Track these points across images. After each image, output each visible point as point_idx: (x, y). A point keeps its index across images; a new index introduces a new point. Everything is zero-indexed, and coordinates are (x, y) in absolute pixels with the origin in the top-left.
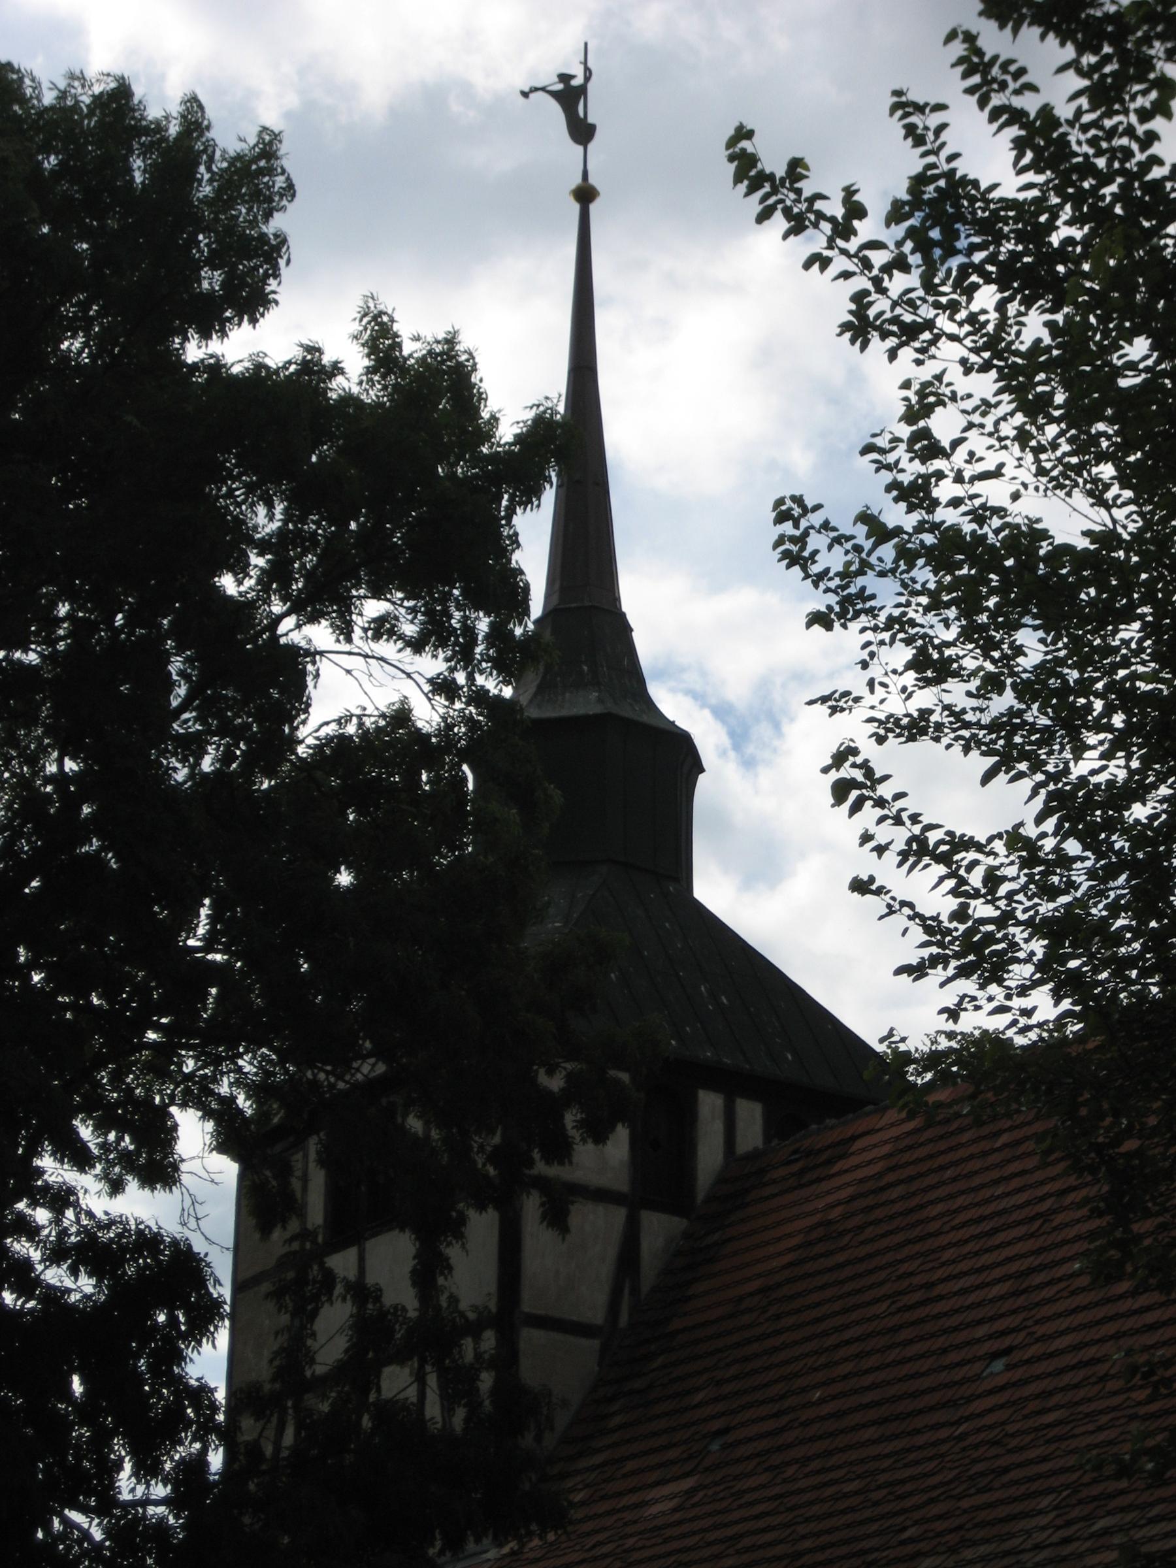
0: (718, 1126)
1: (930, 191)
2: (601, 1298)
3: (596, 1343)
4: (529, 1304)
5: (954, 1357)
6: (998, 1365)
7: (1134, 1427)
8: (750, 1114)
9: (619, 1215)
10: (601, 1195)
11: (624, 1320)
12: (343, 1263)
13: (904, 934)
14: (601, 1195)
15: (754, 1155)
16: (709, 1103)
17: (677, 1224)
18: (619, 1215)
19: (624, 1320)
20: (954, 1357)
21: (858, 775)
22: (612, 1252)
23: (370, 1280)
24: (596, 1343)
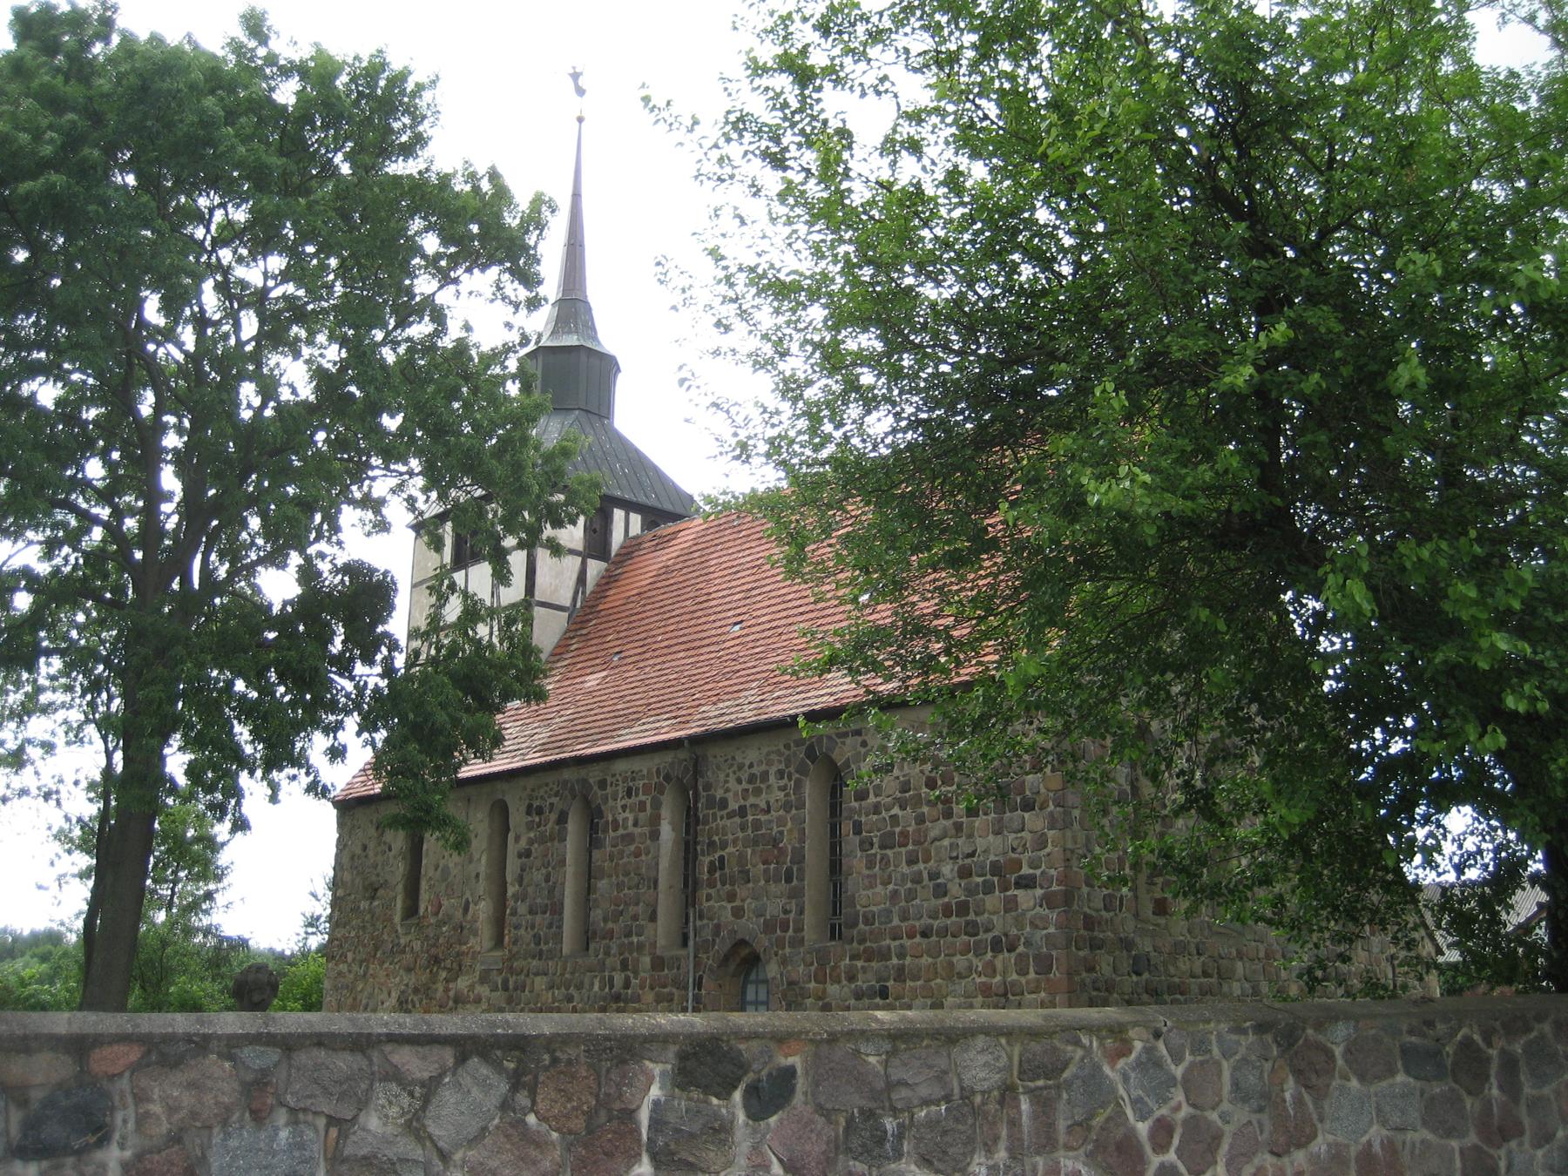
0: (622, 524)
1: (732, 118)
2: (570, 595)
3: (566, 615)
4: (538, 596)
5: (718, 624)
6: (737, 628)
7: (793, 654)
8: (636, 520)
9: (579, 560)
10: (572, 552)
11: (578, 605)
12: (459, 577)
13: (687, 421)
14: (572, 552)
15: (637, 537)
16: (618, 514)
17: (604, 565)
18: (579, 560)
19: (578, 605)
20: (718, 624)
21: (689, 376)
22: (575, 576)
23: (470, 590)
24: (566, 615)
